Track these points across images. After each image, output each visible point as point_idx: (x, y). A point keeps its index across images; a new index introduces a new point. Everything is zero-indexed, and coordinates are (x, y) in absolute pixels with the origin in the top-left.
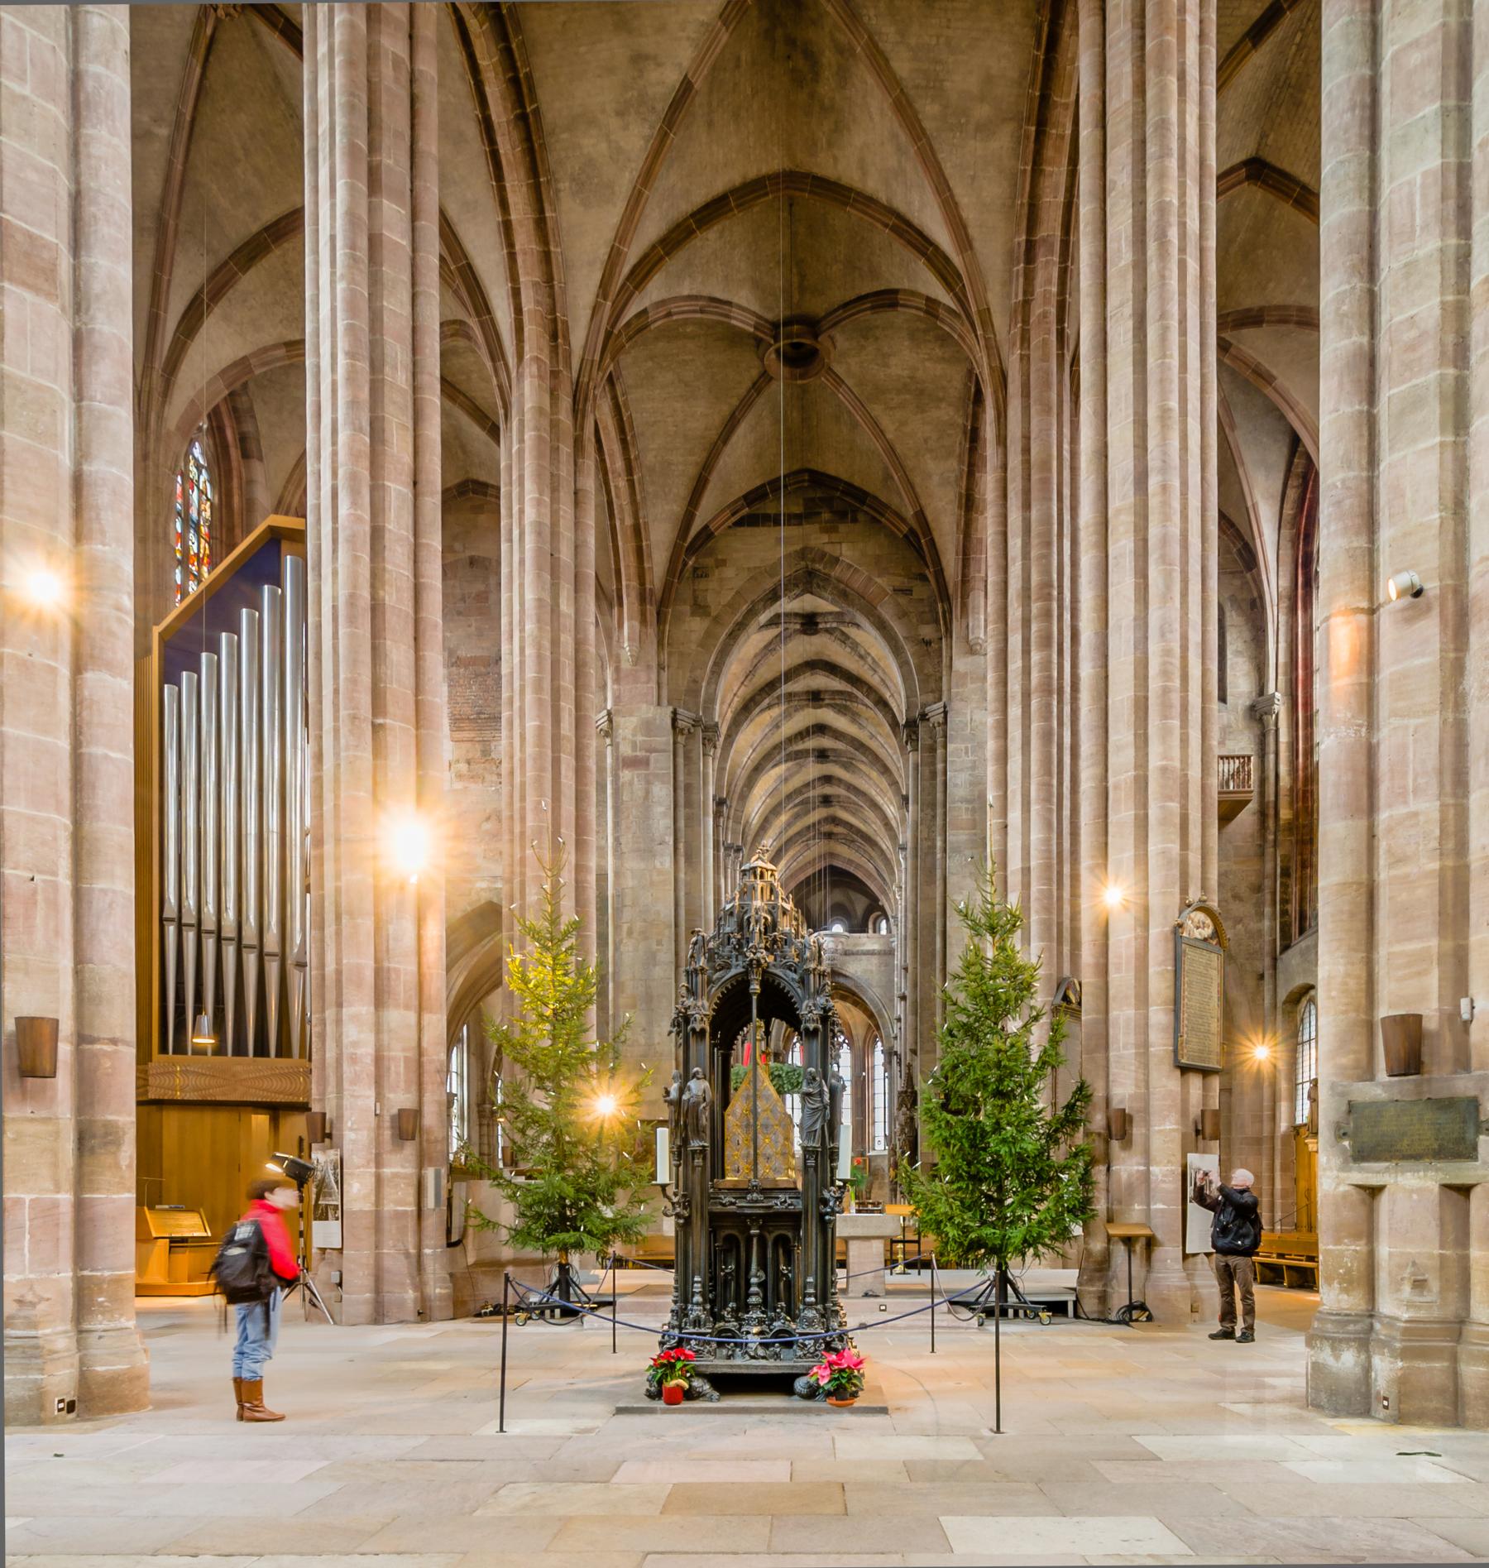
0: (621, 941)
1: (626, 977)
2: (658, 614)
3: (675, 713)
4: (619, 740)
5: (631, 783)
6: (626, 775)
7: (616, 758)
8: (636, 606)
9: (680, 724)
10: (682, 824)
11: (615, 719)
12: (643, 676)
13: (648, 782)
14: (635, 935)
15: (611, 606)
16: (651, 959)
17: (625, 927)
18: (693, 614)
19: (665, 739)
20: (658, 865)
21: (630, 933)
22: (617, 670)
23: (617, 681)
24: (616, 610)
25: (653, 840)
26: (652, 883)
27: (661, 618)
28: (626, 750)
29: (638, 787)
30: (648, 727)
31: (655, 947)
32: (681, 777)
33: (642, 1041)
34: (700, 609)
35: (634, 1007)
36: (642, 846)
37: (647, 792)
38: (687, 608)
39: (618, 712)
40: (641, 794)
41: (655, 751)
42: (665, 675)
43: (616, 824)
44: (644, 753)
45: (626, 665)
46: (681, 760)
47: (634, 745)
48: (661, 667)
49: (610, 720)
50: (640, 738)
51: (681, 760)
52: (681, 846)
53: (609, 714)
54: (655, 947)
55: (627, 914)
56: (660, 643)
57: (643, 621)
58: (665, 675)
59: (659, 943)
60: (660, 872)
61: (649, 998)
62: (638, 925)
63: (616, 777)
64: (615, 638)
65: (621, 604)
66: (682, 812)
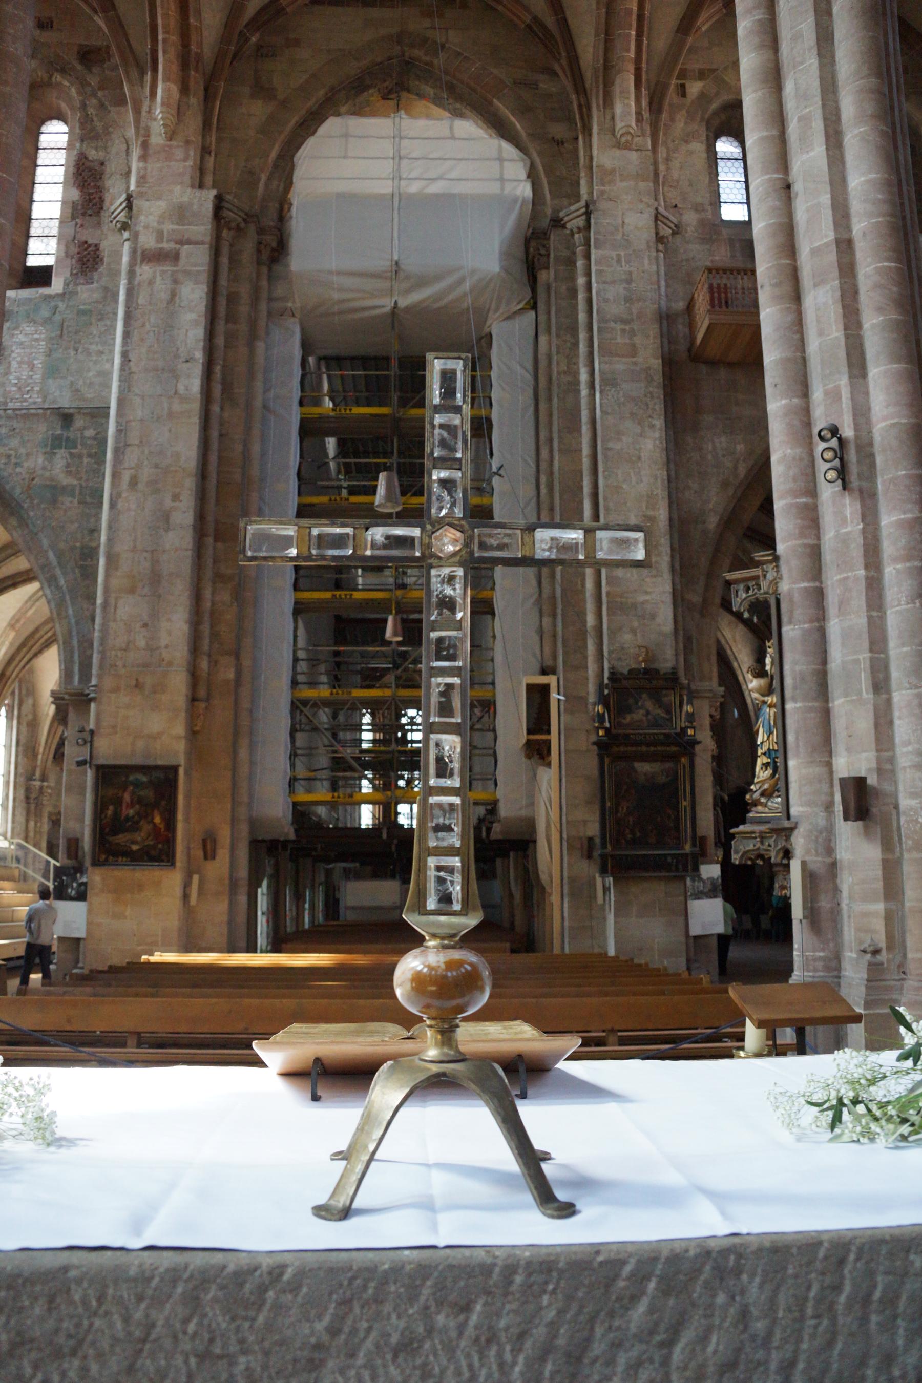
0: (119, 495)
1: (123, 547)
2: (206, 89)
3: (219, 199)
4: (139, 228)
5: (151, 283)
6: (145, 271)
7: (134, 252)
8: (175, 67)
9: (225, 213)
10: (220, 341)
11: (136, 203)
12: (179, 153)
13: (176, 281)
14: (140, 486)
15: (142, 73)
16: (164, 518)
17: (126, 477)
18: (253, 96)
19: (203, 229)
20: (181, 388)
21: (134, 482)
22: (145, 145)
23: (143, 158)
24: (148, 78)
25: (177, 356)
26: (171, 415)
27: (208, 96)
28: (148, 241)
29: (162, 287)
30: (181, 213)
31: (168, 503)
32: (223, 282)
33: (142, 643)
34: (262, 90)
35: (132, 591)
36: (160, 364)
37: (173, 295)
38: (247, 90)
39: (141, 195)
40: (165, 296)
41: (189, 242)
42: (210, 161)
43: (126, 335)
44: (172, 245)
45: (157, 138)
46: (224, 260)
47: (160, 236)
48: (205, 151)
49: (130, 207)
50: (168, 227)
51: (224, 260)
52: (218, 369)
53: (129, 198)
54: (168, 503)
55: (132, 457)
56: (206, 125)
57: (185, 89)
58: (210, 161)
59: (176, 497)
60: (184, 399)
61: (155, 578)
62: (146, 473)
63: (131, 273)
64: (145, 108)
65: (155, 70)
66: (221, 327)
